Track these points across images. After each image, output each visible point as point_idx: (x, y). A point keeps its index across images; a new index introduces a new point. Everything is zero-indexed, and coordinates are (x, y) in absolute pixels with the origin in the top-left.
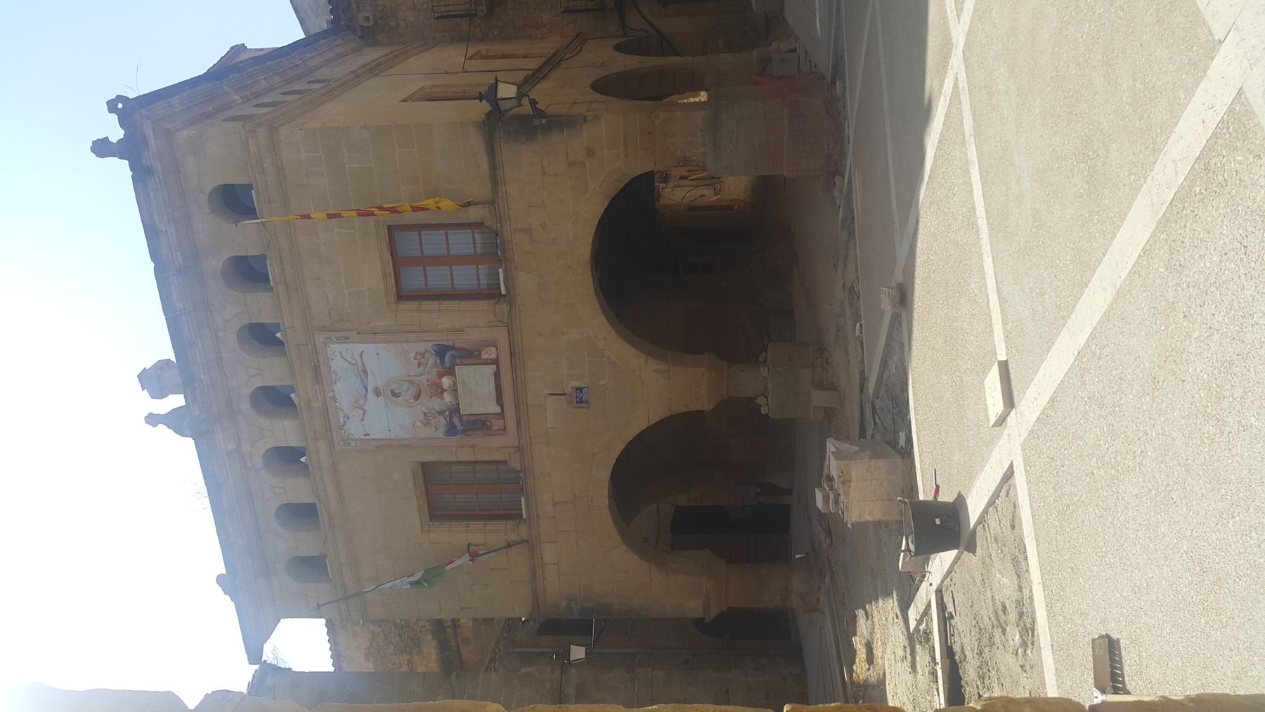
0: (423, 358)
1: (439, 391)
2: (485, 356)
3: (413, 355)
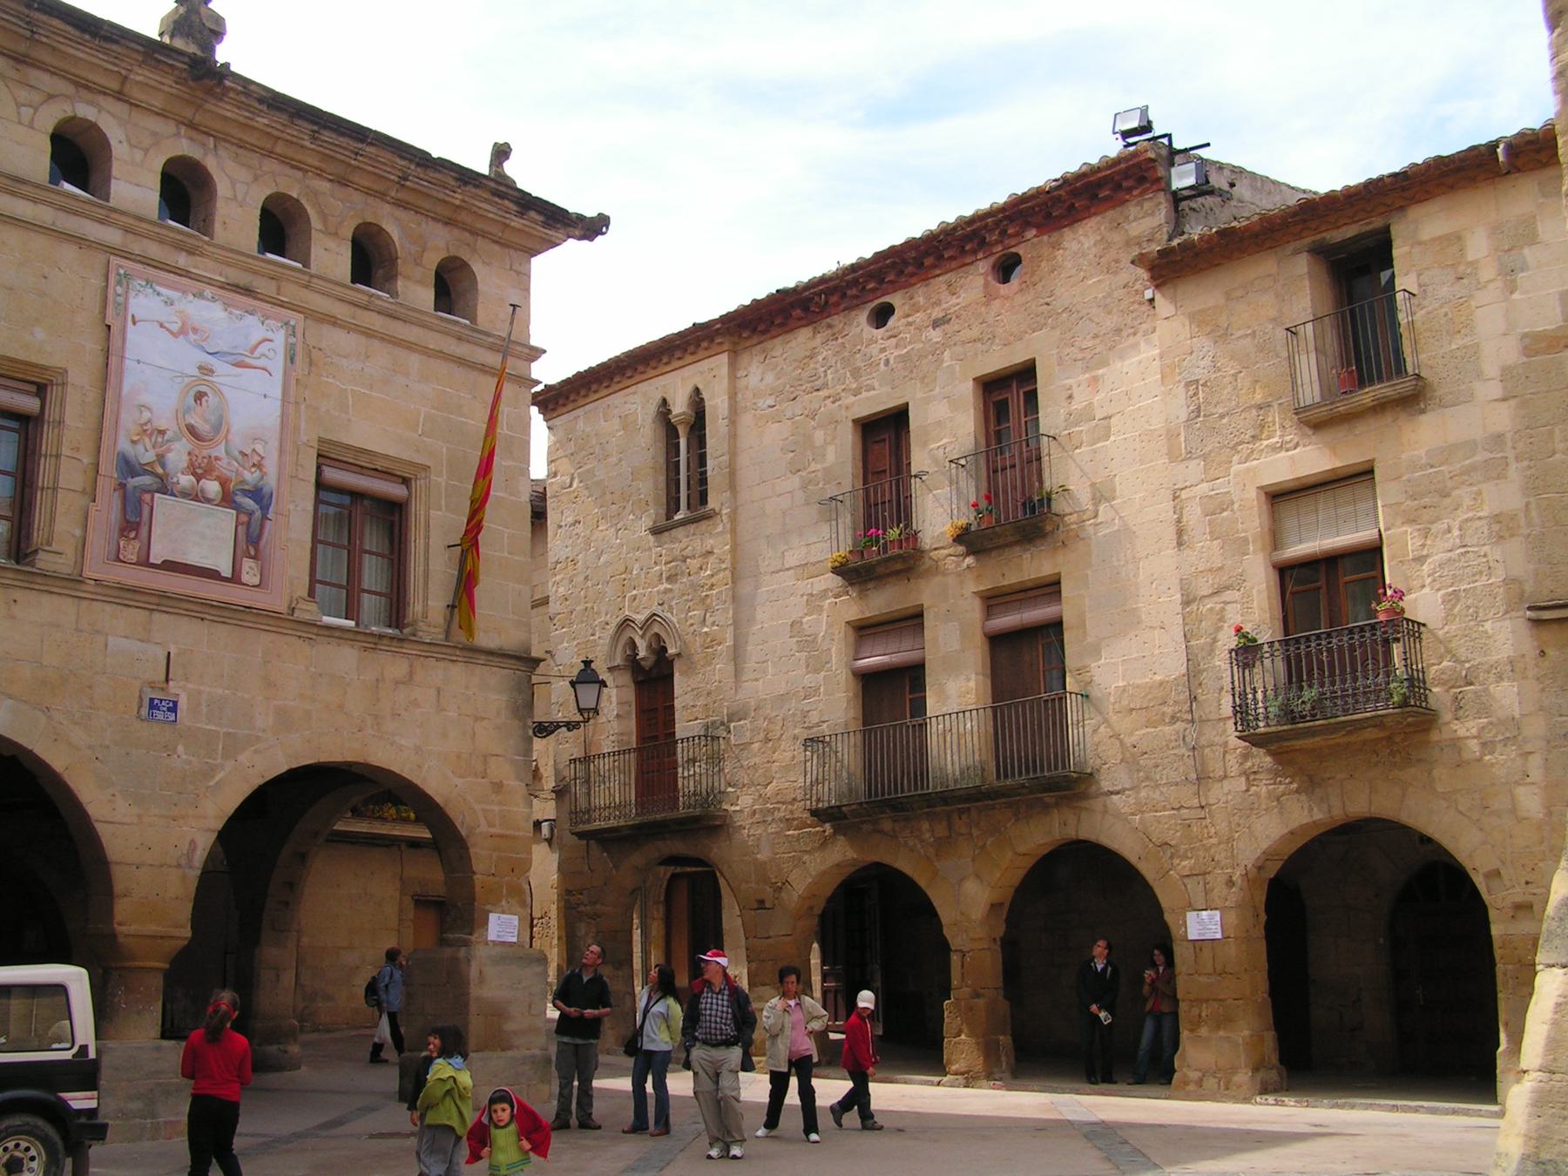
0: (254, 465)
1: (200, 470)
2: (248, 565)
3: (259, 448)
